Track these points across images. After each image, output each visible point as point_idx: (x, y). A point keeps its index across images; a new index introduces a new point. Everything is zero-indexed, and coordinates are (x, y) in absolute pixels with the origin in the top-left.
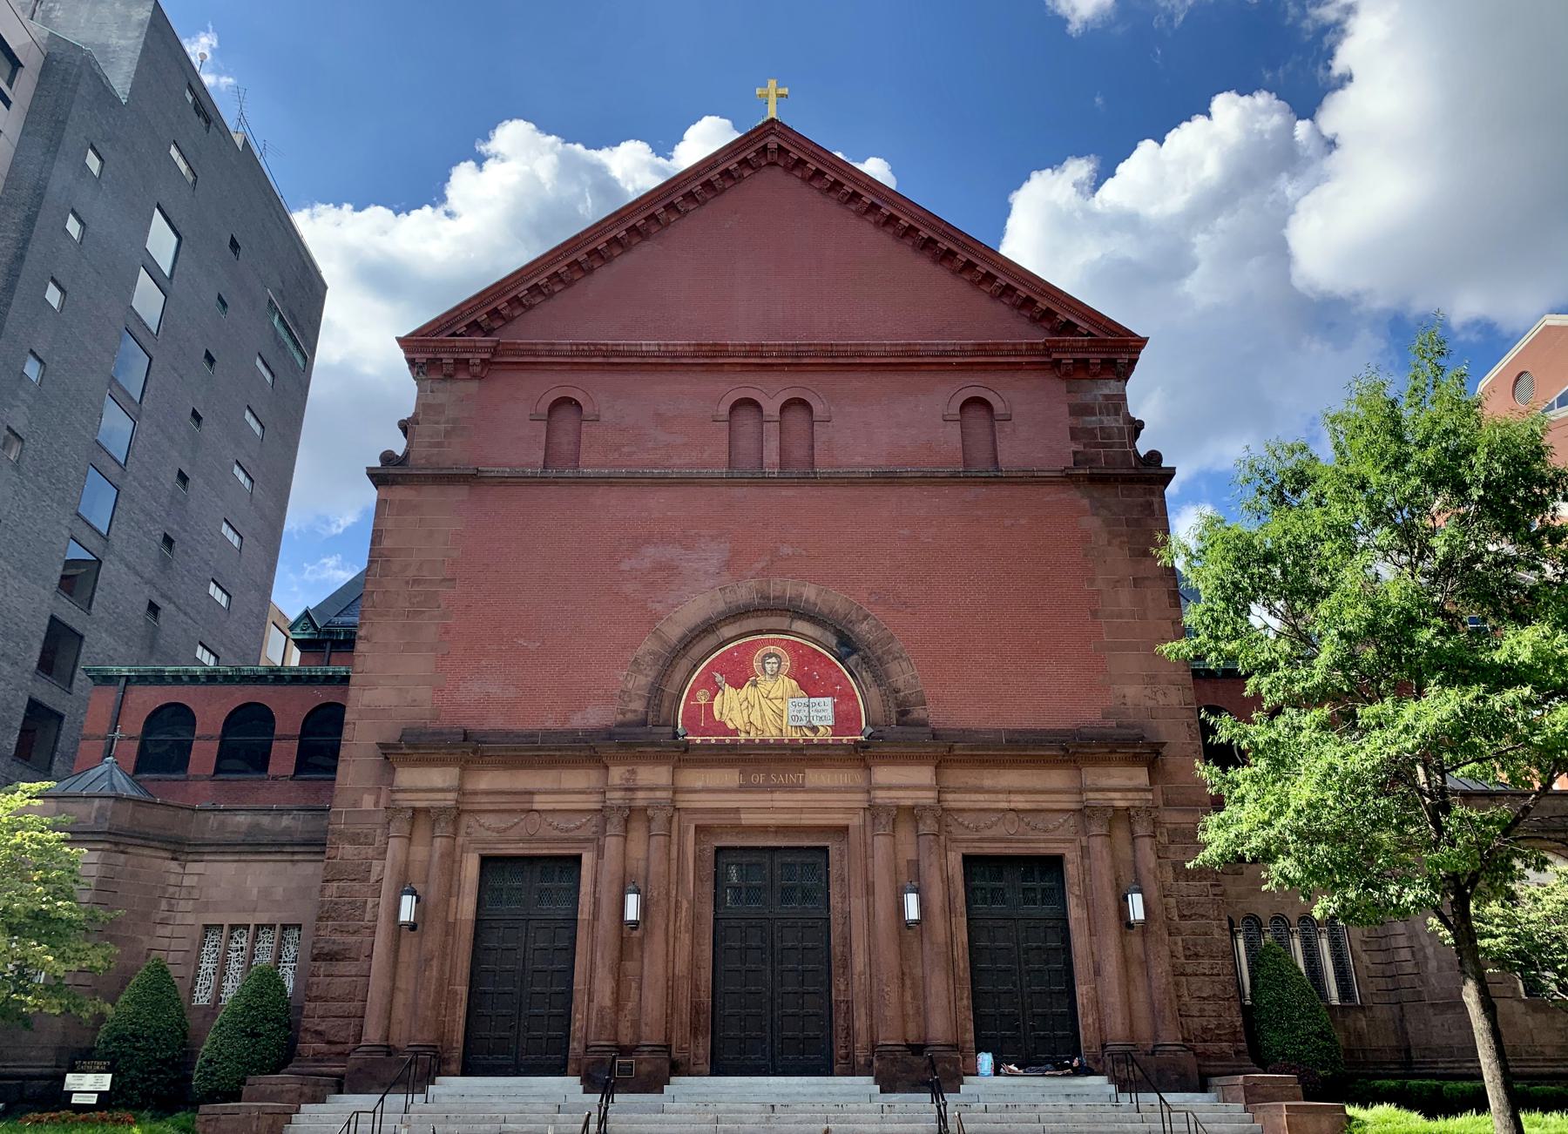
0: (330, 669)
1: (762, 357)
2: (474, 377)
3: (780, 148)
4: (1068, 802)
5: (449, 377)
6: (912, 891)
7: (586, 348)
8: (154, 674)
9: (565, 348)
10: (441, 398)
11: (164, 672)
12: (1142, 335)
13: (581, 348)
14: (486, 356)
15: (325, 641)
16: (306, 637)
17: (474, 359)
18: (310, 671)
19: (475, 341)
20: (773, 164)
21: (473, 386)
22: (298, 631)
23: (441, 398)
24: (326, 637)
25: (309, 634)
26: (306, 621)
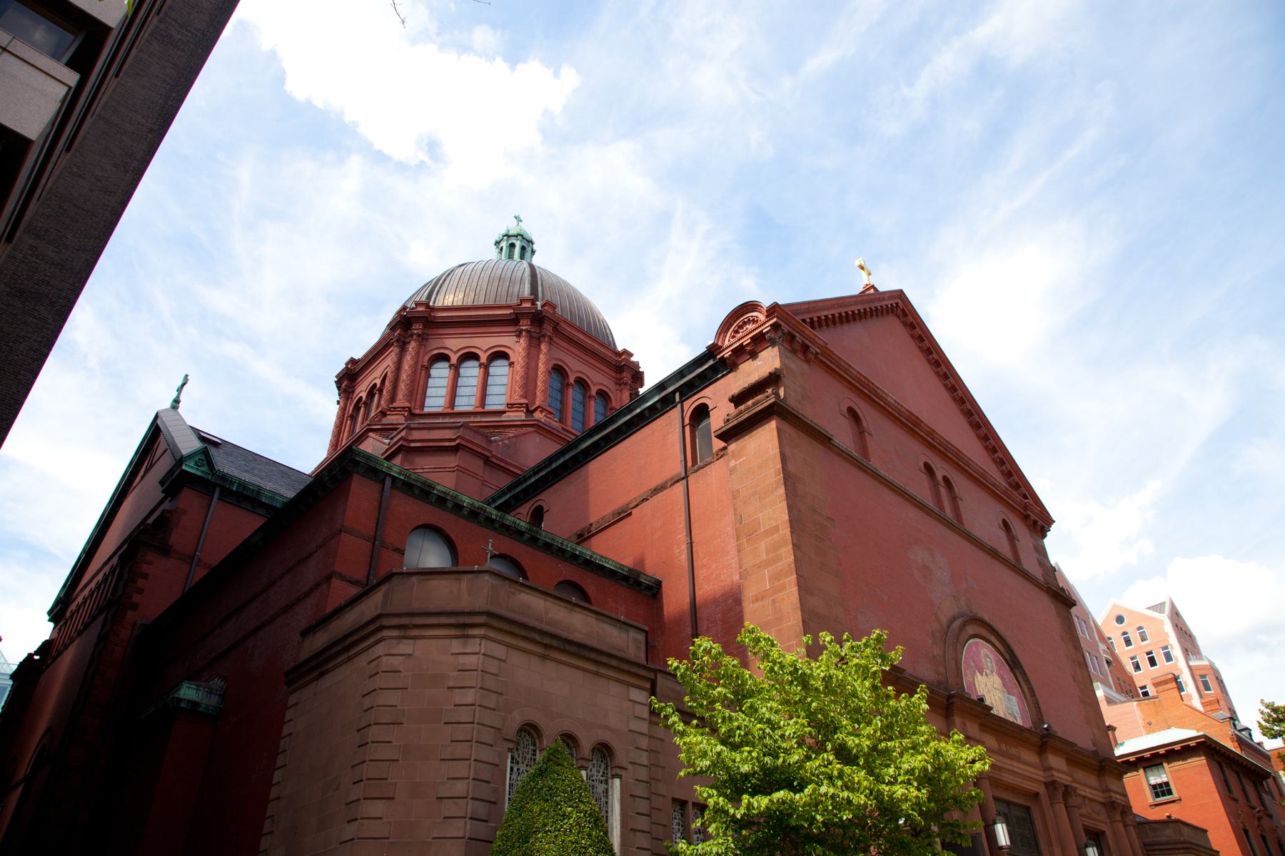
0: (579, 548)
1: (933, 440)
2: (808, 361)
3: (903, 310)
4: (1098, 796)
5: (794, 351)
6: (1001, 848)
7: (864, 380)
8: (423, 486)
9: (854, 372)
10: (792, 365)
11: (434, 488)
12: (1054, 519)
13: (861, 378)
14: (818, 351)
15: (215, 485)
16: (199, 473)
17: (814, 349)
18: (562, 544)
19: (816, 336)
20: (898, 317)
21: (806, 366)
22: (192, 464)
23: (792, 365)
24: (218, 482)
25: (203, 472)
26: (203, 458)
